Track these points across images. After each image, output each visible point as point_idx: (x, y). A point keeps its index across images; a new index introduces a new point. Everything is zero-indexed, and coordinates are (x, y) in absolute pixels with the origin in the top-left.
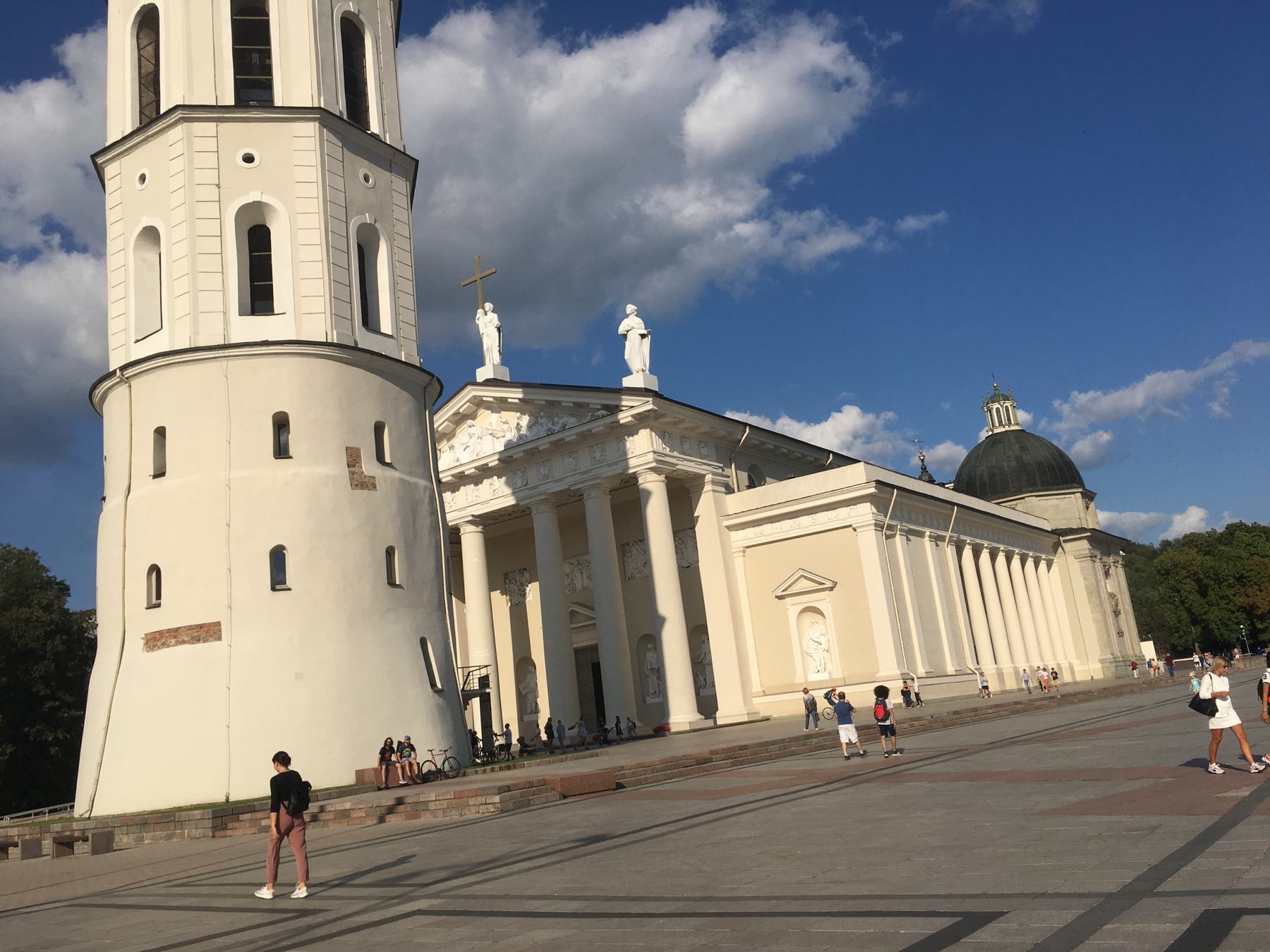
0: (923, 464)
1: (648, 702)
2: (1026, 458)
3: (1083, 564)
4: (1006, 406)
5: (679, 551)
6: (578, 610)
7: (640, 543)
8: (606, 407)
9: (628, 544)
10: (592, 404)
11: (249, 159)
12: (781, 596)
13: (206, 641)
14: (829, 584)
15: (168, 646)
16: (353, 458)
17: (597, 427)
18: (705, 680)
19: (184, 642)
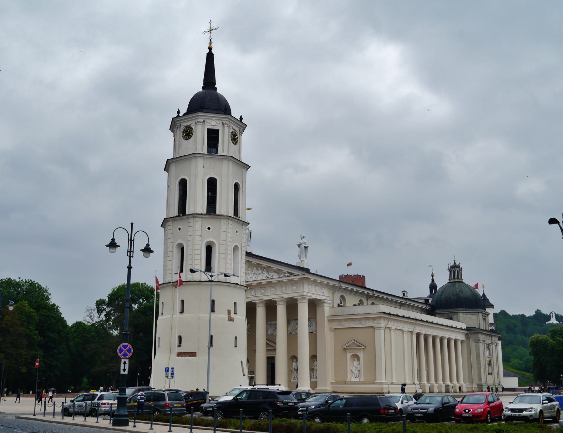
0: (433, 278)
1: (291, 381)
2: (461, 295)
3: (476, 343)
4: (458, 271)
5: (310, 326)
6: (269, 343)
7: (295, 320)
8: (289, 273)
9: (290, 320)
10: (284, 271)
11: (209, 228)
12: (345, 349)
13: (192, 357)
14: (363, 347)
15: (183, 357)
16: (229, 312)
17: (285, 279)
18: (314, 375)
19: (187, 356)
